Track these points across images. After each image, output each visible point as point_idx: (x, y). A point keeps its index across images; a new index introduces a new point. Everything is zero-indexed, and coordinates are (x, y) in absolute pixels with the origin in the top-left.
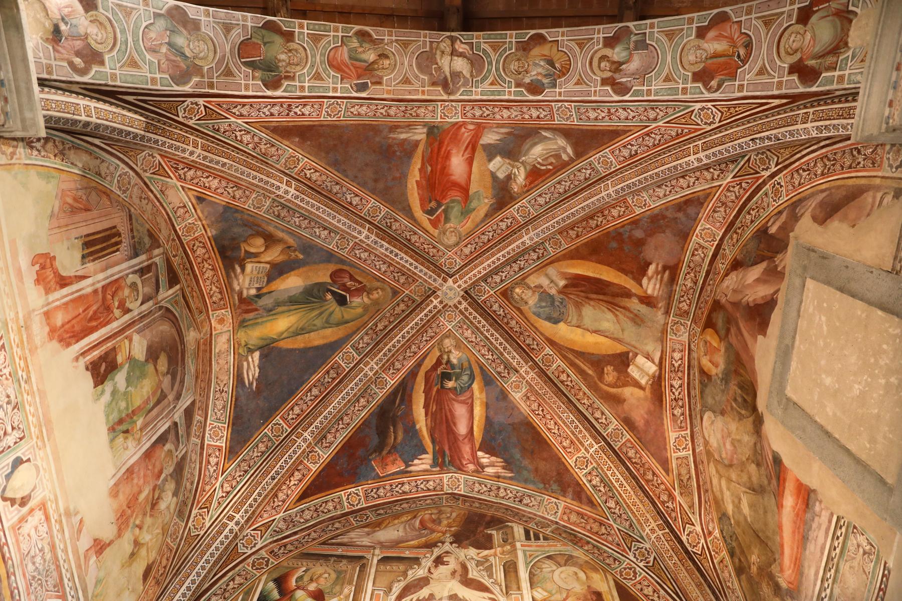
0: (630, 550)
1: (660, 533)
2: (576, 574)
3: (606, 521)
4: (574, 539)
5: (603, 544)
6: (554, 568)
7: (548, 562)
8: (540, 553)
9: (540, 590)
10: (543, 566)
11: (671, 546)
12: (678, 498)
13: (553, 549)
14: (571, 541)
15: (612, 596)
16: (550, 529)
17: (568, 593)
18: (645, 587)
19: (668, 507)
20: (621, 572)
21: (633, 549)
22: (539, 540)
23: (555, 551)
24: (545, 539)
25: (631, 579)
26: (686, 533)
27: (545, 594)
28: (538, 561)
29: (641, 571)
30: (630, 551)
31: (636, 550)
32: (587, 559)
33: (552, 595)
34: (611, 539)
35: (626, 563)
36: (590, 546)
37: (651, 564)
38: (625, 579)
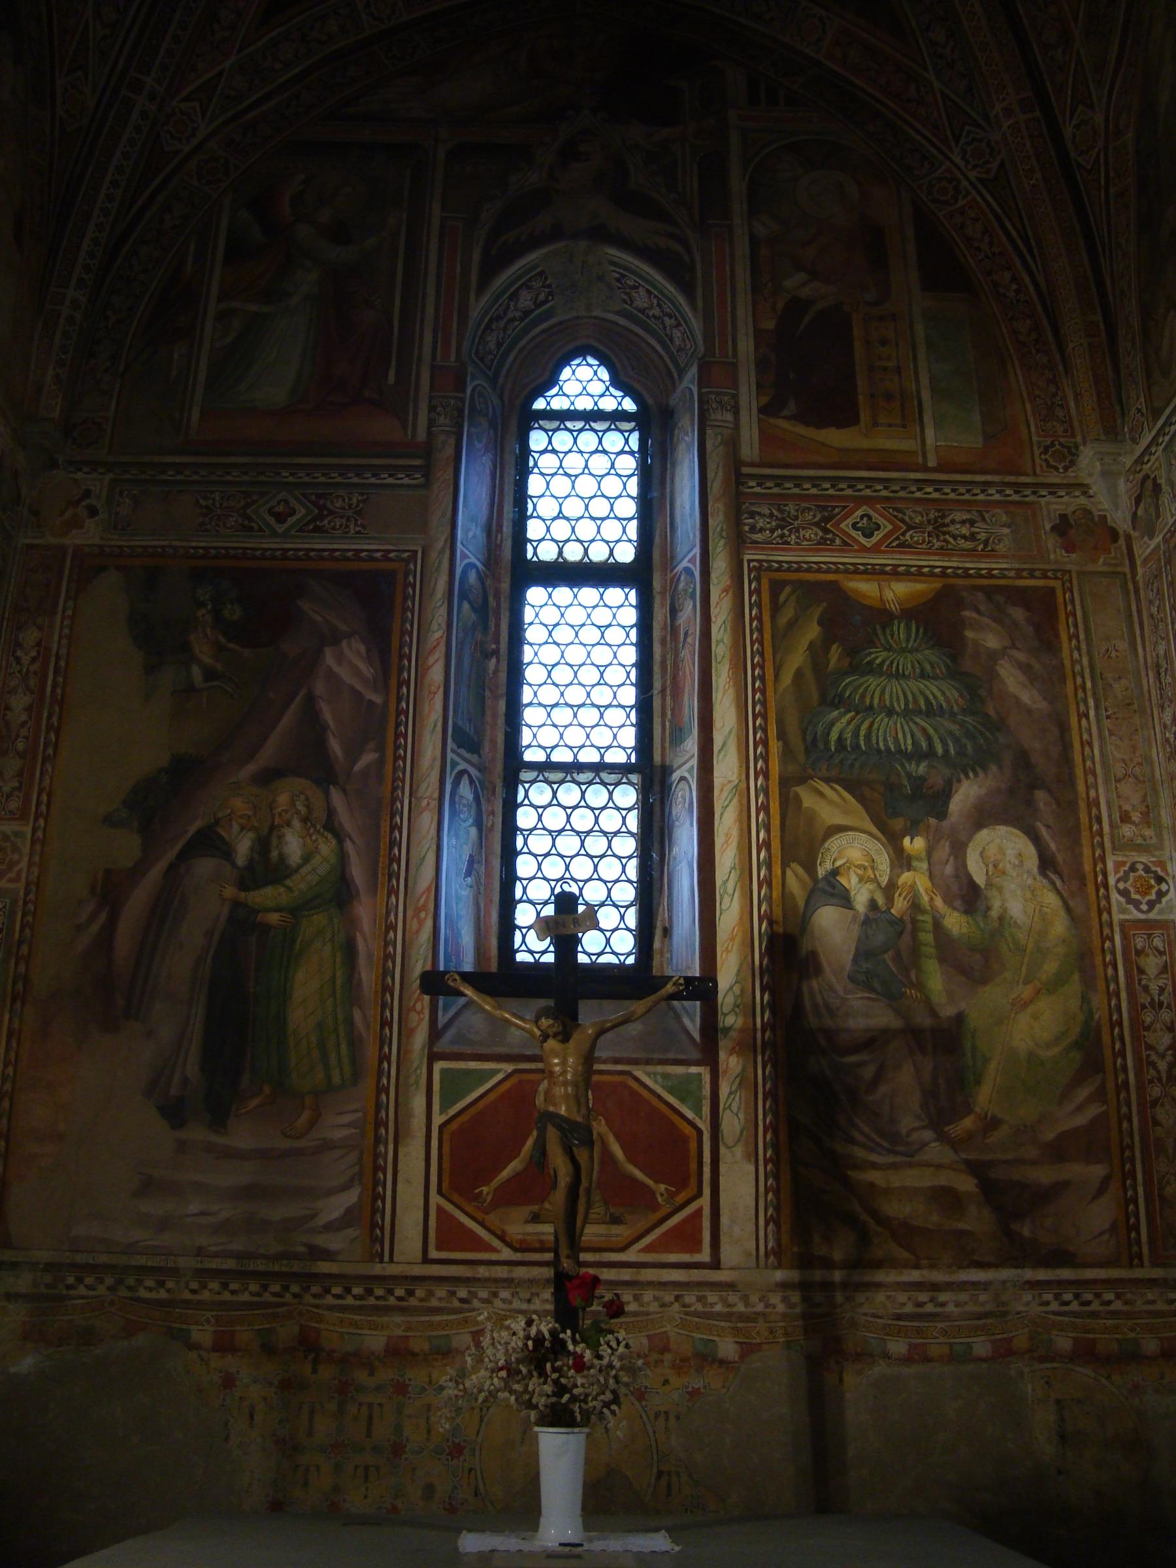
21: (962, 141)
29: (970, 188)
30: (957, 146)
35: (944, 168)
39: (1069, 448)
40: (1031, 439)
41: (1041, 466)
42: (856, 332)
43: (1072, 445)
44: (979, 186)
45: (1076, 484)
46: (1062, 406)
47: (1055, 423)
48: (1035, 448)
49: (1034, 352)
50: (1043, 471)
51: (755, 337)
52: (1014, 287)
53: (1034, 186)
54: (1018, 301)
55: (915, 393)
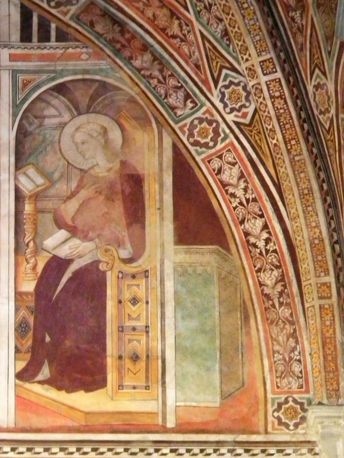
0: (216, 83)
1: (264, 79)
2: (105, 131)
3: (182, 10)
4: (118, 37)
5: (171, 56)
6: (67, 117)
7: (59, 101)
8: (44, 77)
9: (31, 171)
10: (46, 113)
11: (276, 109)
12: (311, 11)
13: (71, 65)
14: (111, 42)
15: (161, 186)
16: (73, 9)
17: (81, 180)
18: (226, 167)
19: (293, 19)
20: (192, 126)
21: (221, 84)
22: (48, 40)
23: (75, 73)
24: (62, 37)
25: (206, 145)
26: (313, 83)
27: (40, 181)
28: (39, 98)
29: (227, 131)
30: (216, 88)
31: (227, 87)
32: (133, 92)
33: (52, 183)
34: (186, 50)
36: (148, 57)
37: (247, 121)
38: (196, 144)
39: (302, 404)
40: (266, 397)
41: (273, 423)
42: (109, 292)
43: (305, 401)
44: (237, 131)
45: (302, 442)
46: (299, 361)
47: (291, 379)
48: (269, 405)
49: (277, 305)
50: (273, 428)
51: (16, 300)
52: (265, 235)
53: (275, 145)
54: (267, 251)
55: (160, 354)
